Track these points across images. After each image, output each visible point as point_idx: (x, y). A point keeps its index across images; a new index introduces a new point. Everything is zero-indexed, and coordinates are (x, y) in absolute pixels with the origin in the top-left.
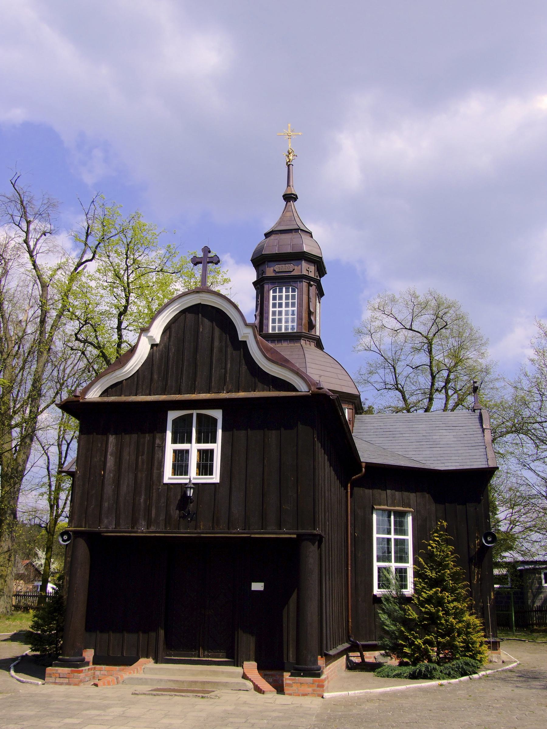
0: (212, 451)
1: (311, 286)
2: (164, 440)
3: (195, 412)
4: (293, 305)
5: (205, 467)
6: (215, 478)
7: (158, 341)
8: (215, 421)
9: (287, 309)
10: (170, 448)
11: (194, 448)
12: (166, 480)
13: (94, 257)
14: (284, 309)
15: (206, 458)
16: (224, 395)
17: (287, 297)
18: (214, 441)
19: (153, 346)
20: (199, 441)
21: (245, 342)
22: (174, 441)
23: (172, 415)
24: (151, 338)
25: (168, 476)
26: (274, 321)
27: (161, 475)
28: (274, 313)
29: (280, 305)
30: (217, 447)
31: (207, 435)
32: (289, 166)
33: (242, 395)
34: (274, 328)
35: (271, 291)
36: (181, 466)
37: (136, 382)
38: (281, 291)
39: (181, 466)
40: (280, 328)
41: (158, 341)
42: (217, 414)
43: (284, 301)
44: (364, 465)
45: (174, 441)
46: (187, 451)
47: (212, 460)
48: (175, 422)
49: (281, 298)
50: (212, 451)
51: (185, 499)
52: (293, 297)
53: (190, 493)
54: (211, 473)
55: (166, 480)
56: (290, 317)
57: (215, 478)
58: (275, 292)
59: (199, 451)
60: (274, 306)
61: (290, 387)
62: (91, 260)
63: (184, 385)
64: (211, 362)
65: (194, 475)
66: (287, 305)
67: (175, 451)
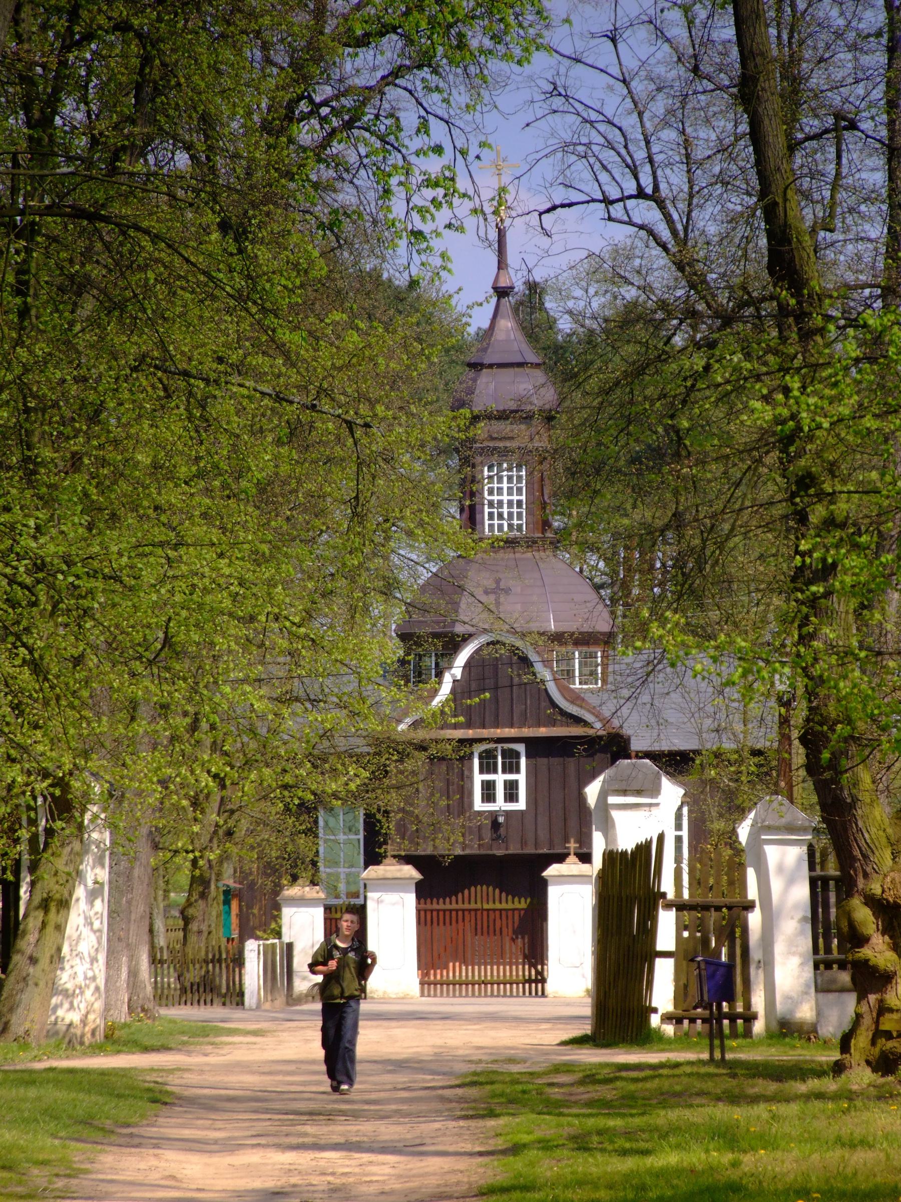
0: (517, 781)
2: (471, 770)
3: (499, 746)
5: (511, 796)
6: (521, 805)
7: (459, 677)
9: (510, 498)
10: (478, 778)
14: (505, 498)
16: (527, 732)
17: (510, 479)
18: (518, 771)
19: (454, 681)
20: (504, 772)
22: (481, 772)
23: (478, 749)
24: (453, 676)
25: (479, 805)
26: (491, 516)
27: (471, 804)
29: (500, 491)
30: (521, 778)
32: (499, 229)
33: (543, 732)
35: (486, 469)
37: (441, 719)
40: (500, 527)
41: (459, 677)
42: (521, 748)
43: (505, 485)
45: (481, 772)
46: (494, 782)
47: (517, 789)
50: (517, 781)
51: (495, 825)
52: (519, 478)
53: (501, 819)
54: (517, 801)
56: (515, 510)
57: (521, 805)
58: (490, 468)
61: (586, 724)
63: (487, 719)
64: (512, 699)
65: (500, 804)
67: (483, 782)
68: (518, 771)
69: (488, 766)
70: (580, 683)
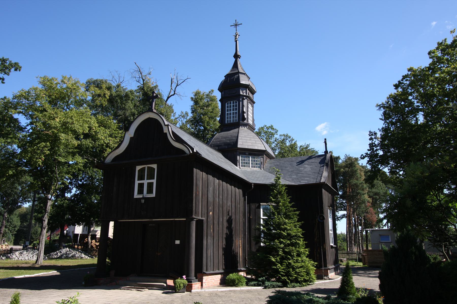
0: (153, 183)
1: (245, 99)
4: (236, 110)
5: (150, 191)
6: (153, 195)
8: (154, 169)
10: (137, 182)
11: (146, 182)
12: (135, 197)
13: (175, 94)
14: (232, 112)
15: (150, 186)
18: (154, 179)
21: (166, 133)
22: (138, 180)
25: (136, 196)
28: (228, 114)
29: (230, 110)
31: (151, 176)
34: (228, 121)
36: (141, 191)
38: (230, 103)
39: (141, 191)
43: (232, 108)
44: (253, 184)
45: (138, 180)
48: (139, 171)
49: (230, 106)
55: (135, 197)
57: (153, 195)
59: (148, 183)
60: (228, 111)
62: (173, 95)
66: (233, 110)
67: (139, 184)
68: (154, 179)
69: (141, 177)
70: (252, 167)
